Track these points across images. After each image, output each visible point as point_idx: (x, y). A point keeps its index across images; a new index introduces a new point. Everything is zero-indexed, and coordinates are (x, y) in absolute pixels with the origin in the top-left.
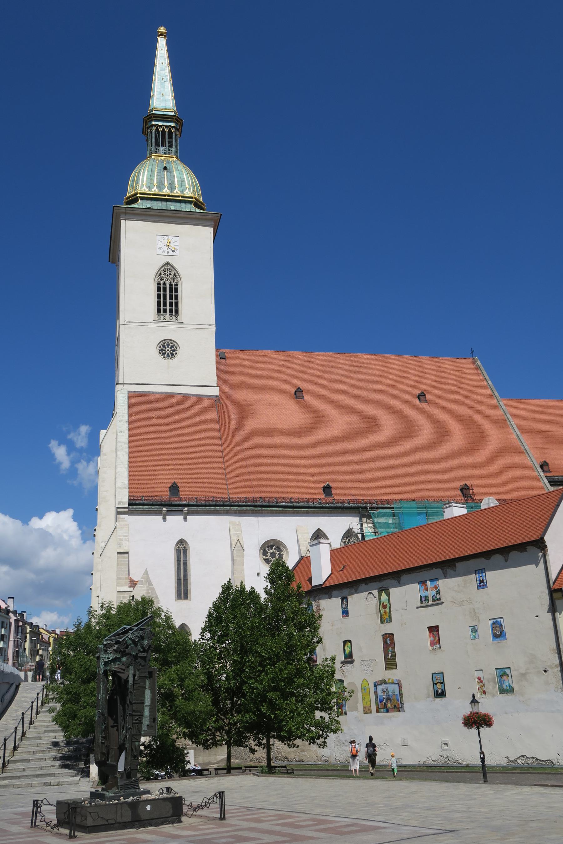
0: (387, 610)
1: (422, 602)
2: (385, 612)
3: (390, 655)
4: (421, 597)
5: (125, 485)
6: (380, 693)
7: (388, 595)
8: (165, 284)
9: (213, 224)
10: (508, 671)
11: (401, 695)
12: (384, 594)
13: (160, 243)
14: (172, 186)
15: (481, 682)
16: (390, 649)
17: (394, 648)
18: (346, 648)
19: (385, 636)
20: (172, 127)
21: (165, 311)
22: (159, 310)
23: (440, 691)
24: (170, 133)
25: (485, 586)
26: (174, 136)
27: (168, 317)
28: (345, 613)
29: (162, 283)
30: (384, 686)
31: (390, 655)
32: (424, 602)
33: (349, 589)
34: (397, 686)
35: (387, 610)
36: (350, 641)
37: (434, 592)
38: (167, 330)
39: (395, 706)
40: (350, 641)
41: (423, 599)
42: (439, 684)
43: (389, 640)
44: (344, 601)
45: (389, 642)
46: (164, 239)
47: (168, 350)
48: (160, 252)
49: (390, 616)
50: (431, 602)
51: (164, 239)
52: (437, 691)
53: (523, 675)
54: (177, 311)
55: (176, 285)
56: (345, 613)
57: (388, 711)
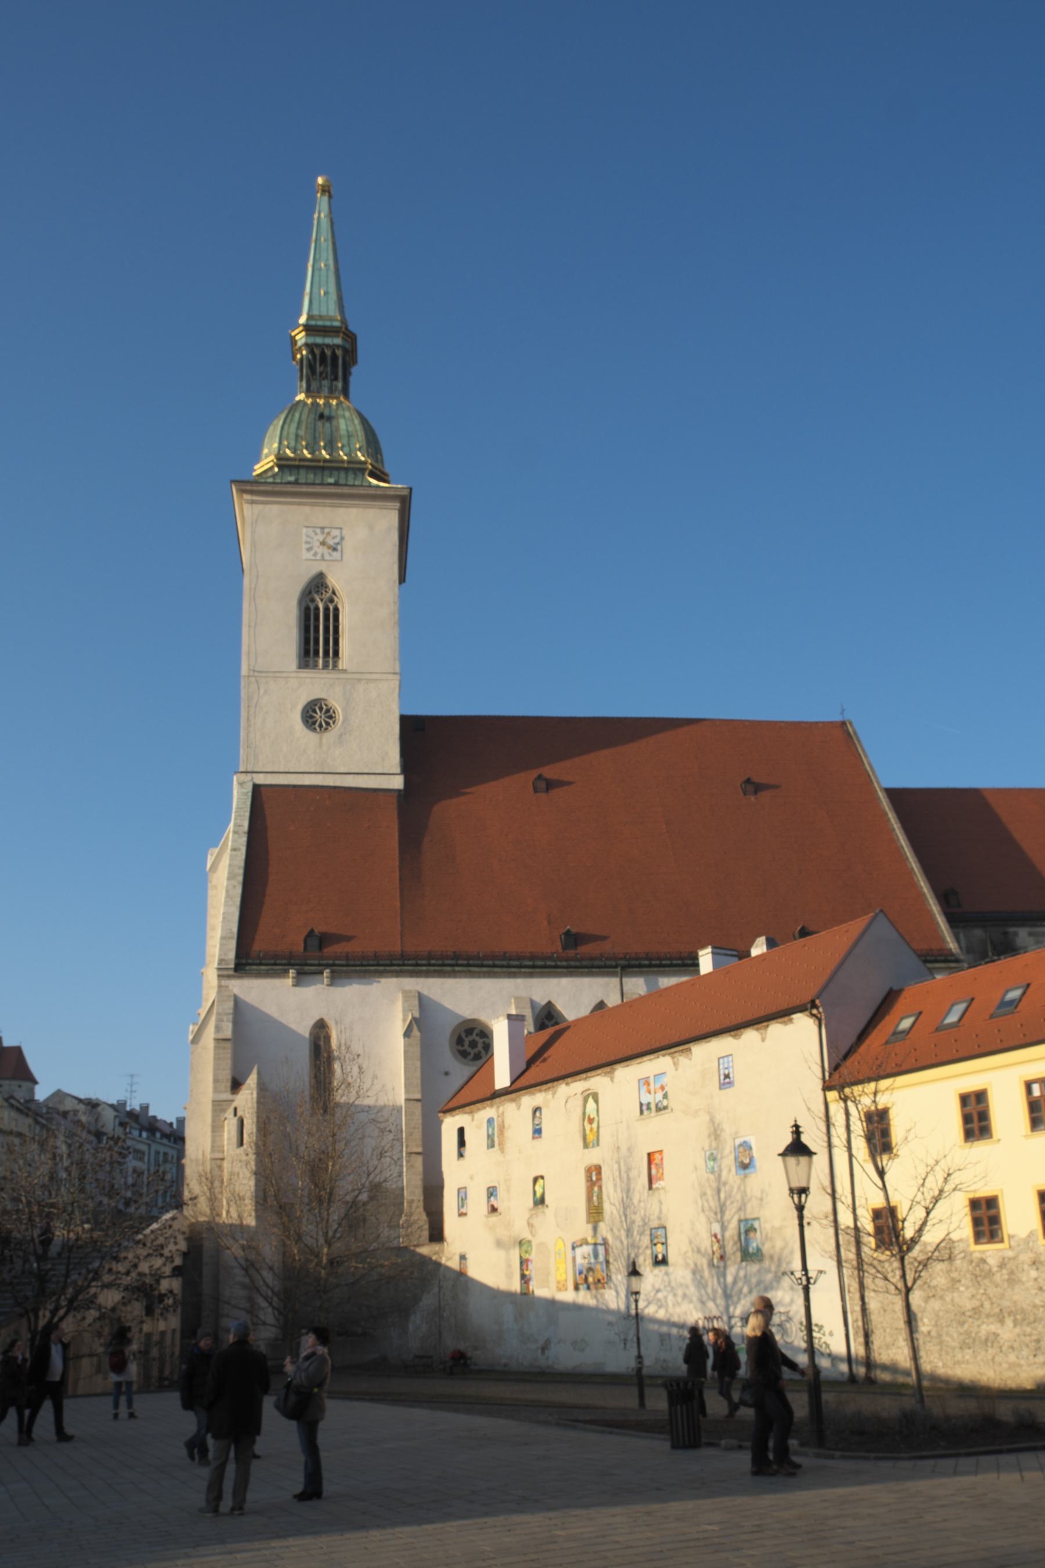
0: (595, 1125)
1: (642, 1112)
2: (591, 1130)
3: (595, 1198)
4: (641, 1105)
5: (232, 933)
7: (596, 1101)
8: (317, 609)
9: (397, 505)
12: (591, 1100)
13: (309, 539)
14: (331, 446)
16: (596, 1189)
17: (600, 1187)
19: (589, 1171)
20: (338, 346)
21: (316, 653)
22: (307, 653)
23: (660, 1257)
24: (334, 357)
25: (731, 1084)
26: (340, 361)
28: (537, 1132)
29: (312, 607)
31: (595, 1198)
32: (645, 1112)
33: (543, 1094)
35: (595, 1125)
37: (659, 1096)
40: (542, 1177)
41: (644, 1108)
42: (659, 1246)
43: (594, 1175)
44: (538, 1114)
45: (594, 1178)
46: (316, 534)
47: (319, 716)
49: (598, 1136)
51: (316, 534)
52: (656, 1257)
54: (336, 653)
55: (336, 609)
56: (537, 1132)
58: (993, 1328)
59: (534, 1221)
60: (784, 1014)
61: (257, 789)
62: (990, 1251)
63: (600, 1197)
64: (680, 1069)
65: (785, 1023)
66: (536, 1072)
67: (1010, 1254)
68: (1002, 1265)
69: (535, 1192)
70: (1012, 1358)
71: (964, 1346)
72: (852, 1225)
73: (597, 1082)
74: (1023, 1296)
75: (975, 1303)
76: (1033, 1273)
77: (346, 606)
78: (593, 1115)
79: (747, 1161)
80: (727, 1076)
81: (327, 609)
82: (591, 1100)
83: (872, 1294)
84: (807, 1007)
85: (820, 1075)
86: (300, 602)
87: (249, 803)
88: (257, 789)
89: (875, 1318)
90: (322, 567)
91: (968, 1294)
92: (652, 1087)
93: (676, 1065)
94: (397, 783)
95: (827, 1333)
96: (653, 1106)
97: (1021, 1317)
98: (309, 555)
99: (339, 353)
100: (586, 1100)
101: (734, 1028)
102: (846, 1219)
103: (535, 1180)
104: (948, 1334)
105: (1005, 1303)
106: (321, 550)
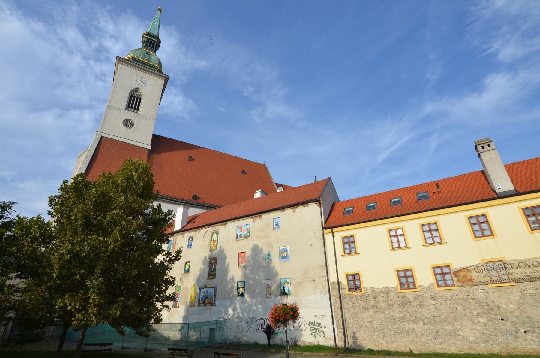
0: (216, 243)
1: (237, 238)
6: (202, 294)
8: (135, 96)
10: (288, 280)
11: (215, 295)
12: (215, 234)
14: (149, 60)
15: (270, 287)
17: (215, 266)
18: (186, 266)
21: (132, 107)
22: (129, 106)
23: (241, 293)
24: (154, 44)
27: (133, 110)
30: (205, 289)
34: (214, 289)
35: (216, 243)
36: (190, 262)
37: (246, 232)
38: (130, 115)
39: (210, 302)
40: (190, 262)
48: (136, 82)
50: (243, 238)
52: (239, 293)
53: (299, 283)
54: (138, 109)
55: (141, 99)
57: (205, 305)
58: (412, 326)
59: (183, 279)
60: (305, 203)
61: (102, 137)
62: (410, 294)
63: (215, 270)
64: (256, 223)
65: (305, 206)
66: (191, 226)
67: (420, 294)
68: (415, 298)
69: (185, 268)
70: (423, 340)
71: (396, 334)
72: (336, 281)
73: (220, 228)
74: (427, 312)
75: (402, 315)
76: (433, 302)
77: (144, 99)
78: (216, 239)
79: (284, 256)
80: (277, 225)
81: (138, 98)
82: (215, 234)
83: (347, 310)
84: (317, 200)
85: (321, 225)
86: (130, 93)
87: (99, 140)
88: (102, 137)
89: (348, 321)
90: (139, 87)
91: (397, 311)
92: (243, 229)
93: (254, 222)
94: (149, 147)
95: (323, 327)
96: (243, 236)
97: (426, 321)
98: (136, 82)
99: (155, 43)
100: (213, 234)
101: (282, 208)
102: (333, 278)
103: (186, 263)
104: (387, 328)
105: (418, 315)
106: (140, 82)
